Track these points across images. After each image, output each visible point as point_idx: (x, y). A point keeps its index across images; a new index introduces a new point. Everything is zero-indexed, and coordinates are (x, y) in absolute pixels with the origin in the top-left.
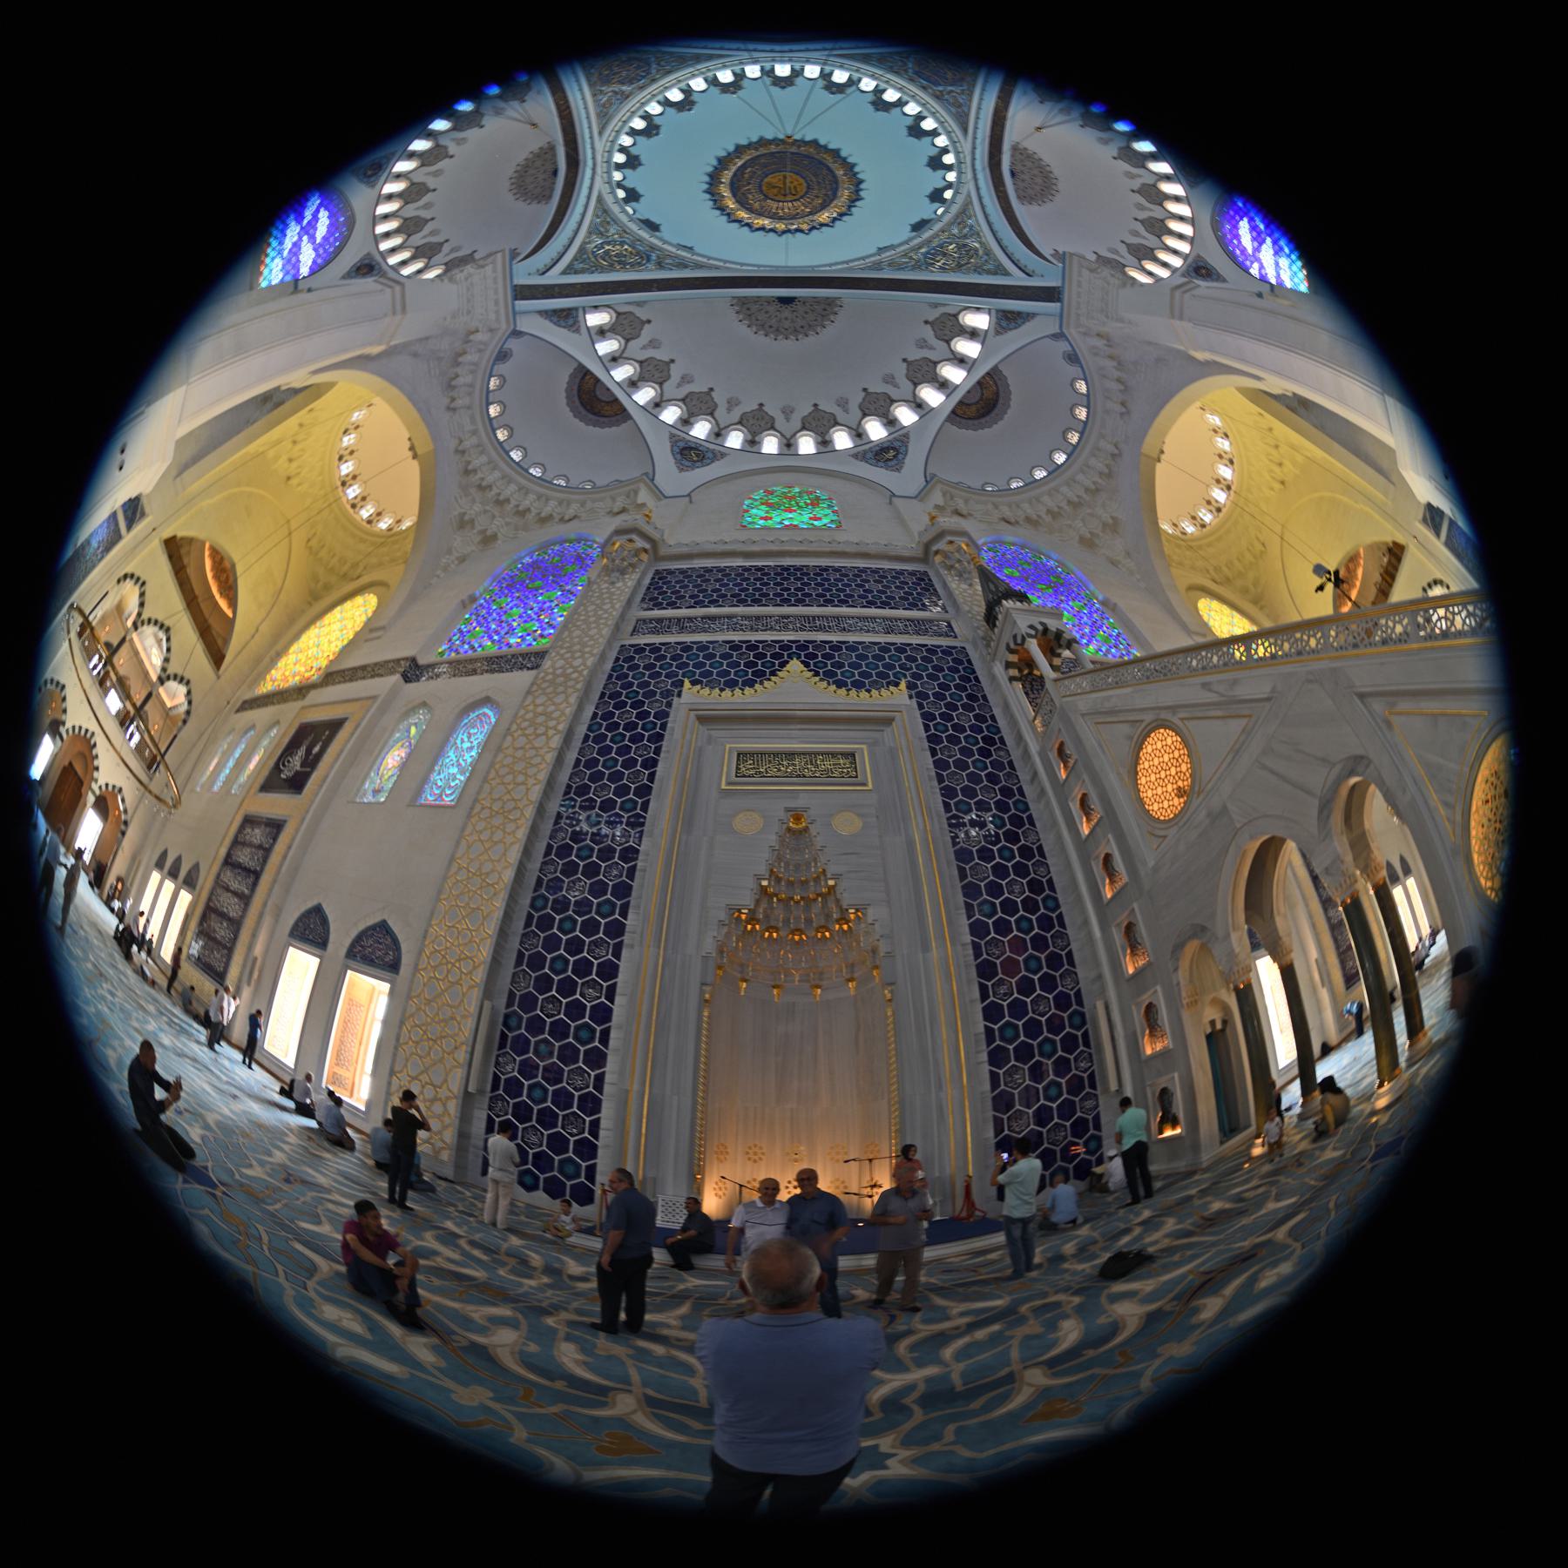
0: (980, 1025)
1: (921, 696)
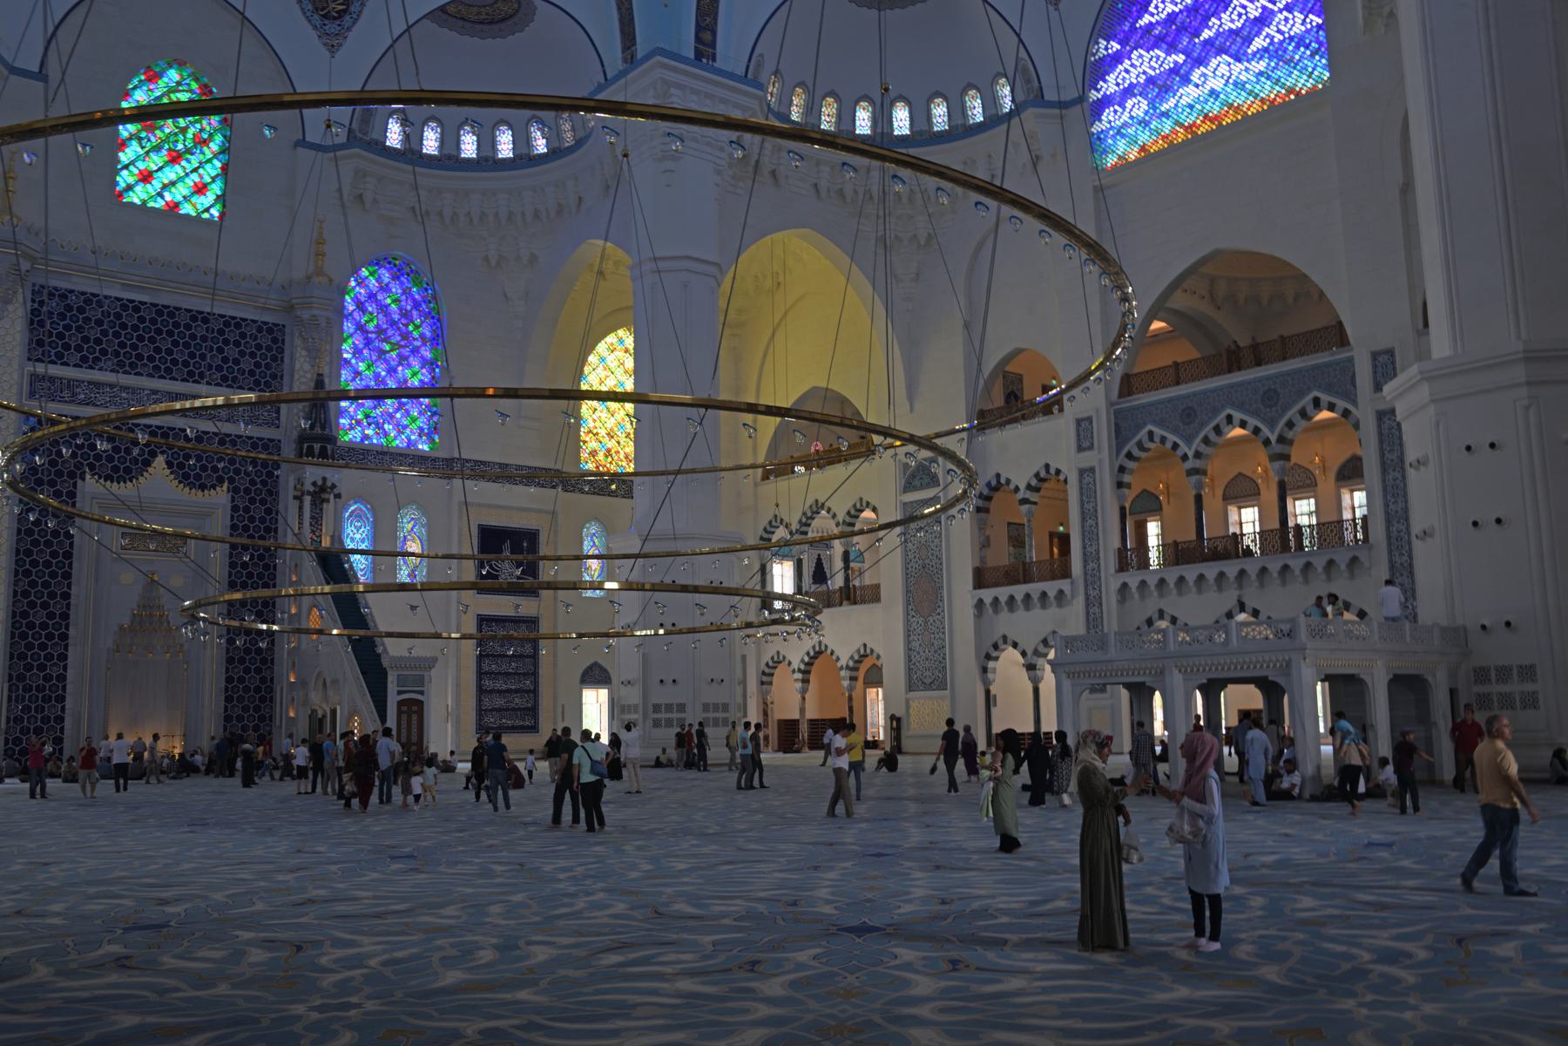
0: (223, 684)
1: (236, 490)
